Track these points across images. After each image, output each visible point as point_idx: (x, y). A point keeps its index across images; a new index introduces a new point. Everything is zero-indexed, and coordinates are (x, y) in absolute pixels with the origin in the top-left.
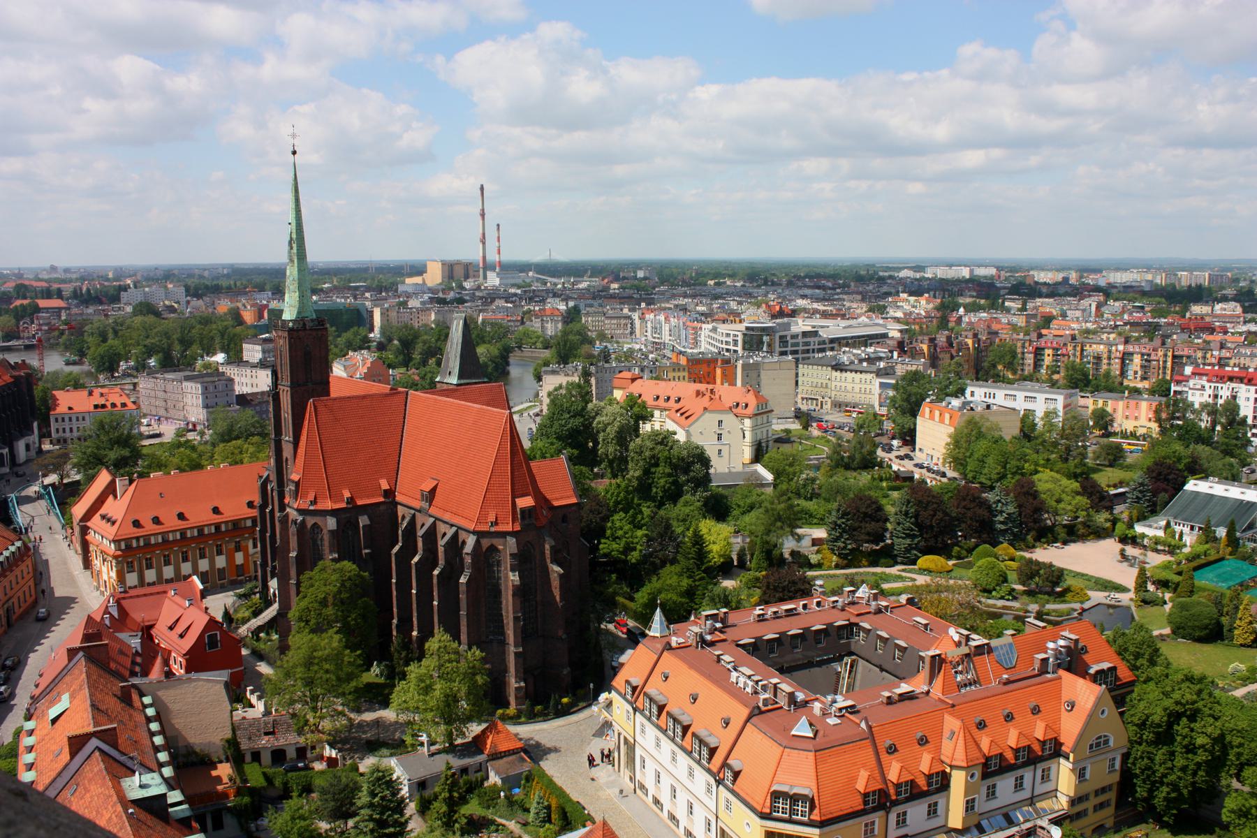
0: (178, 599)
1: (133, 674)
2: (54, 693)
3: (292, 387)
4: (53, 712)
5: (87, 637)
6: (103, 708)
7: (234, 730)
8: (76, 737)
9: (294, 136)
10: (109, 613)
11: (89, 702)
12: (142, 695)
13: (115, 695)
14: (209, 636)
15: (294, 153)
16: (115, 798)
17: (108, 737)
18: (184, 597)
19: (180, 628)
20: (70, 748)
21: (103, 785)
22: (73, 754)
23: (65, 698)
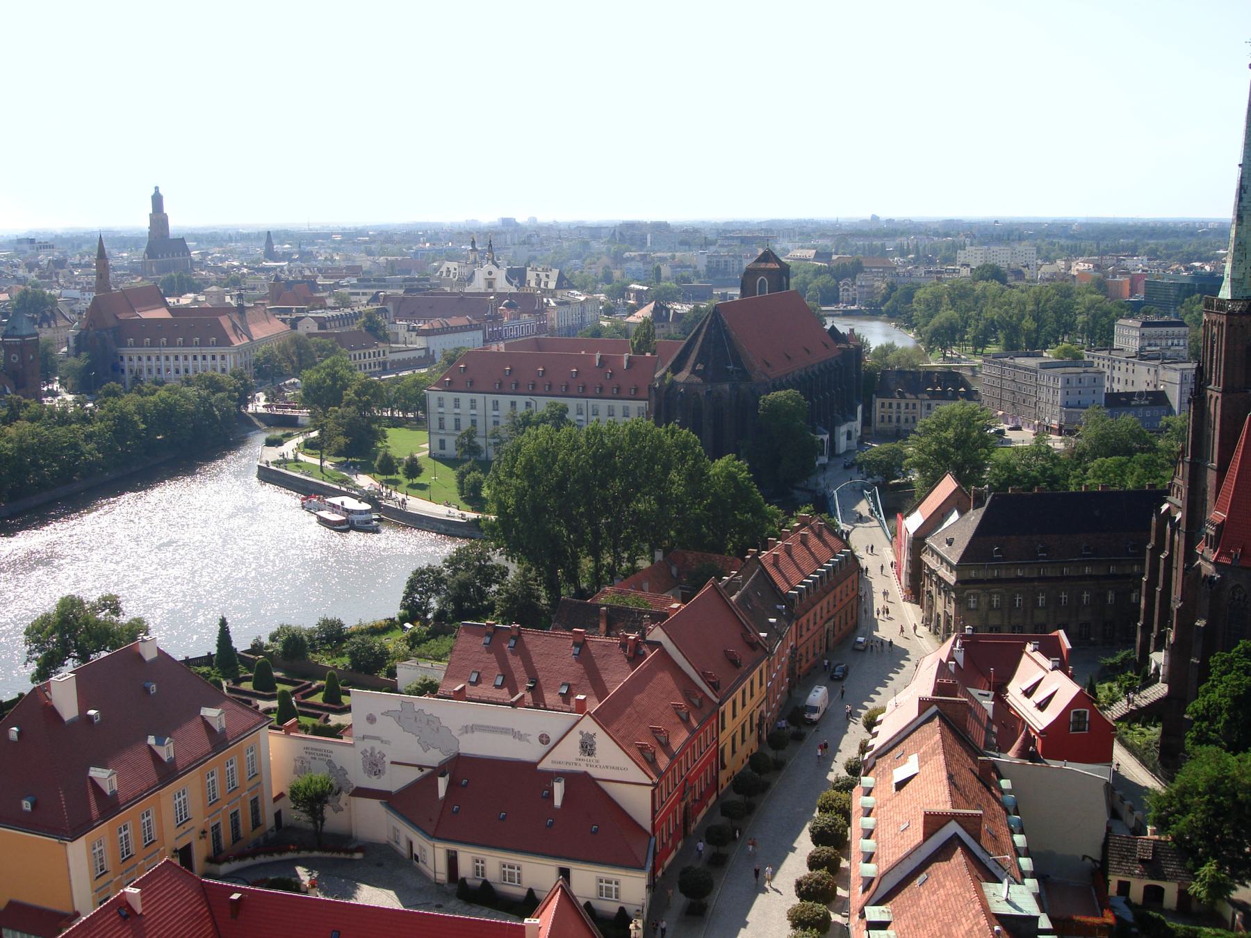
0: (1038, 656)
1: (988, 745)
2: (897, 751)
3: (1224, 392)
4: (900, 774)
5: (939, 689)
6: (960, 783)
7: (1105, 845)
8: (934, 815)
10: (954, 659)
11: (944, 774)
12: (1000, 777)
13: (972, 771)
14: (1074, 713)
16: (978, 907)
18: (1048, 655)
19: (1039, 696)
20: (925, 827)
21: (962, 885)
22: (927, 835)
23: (913, 760)
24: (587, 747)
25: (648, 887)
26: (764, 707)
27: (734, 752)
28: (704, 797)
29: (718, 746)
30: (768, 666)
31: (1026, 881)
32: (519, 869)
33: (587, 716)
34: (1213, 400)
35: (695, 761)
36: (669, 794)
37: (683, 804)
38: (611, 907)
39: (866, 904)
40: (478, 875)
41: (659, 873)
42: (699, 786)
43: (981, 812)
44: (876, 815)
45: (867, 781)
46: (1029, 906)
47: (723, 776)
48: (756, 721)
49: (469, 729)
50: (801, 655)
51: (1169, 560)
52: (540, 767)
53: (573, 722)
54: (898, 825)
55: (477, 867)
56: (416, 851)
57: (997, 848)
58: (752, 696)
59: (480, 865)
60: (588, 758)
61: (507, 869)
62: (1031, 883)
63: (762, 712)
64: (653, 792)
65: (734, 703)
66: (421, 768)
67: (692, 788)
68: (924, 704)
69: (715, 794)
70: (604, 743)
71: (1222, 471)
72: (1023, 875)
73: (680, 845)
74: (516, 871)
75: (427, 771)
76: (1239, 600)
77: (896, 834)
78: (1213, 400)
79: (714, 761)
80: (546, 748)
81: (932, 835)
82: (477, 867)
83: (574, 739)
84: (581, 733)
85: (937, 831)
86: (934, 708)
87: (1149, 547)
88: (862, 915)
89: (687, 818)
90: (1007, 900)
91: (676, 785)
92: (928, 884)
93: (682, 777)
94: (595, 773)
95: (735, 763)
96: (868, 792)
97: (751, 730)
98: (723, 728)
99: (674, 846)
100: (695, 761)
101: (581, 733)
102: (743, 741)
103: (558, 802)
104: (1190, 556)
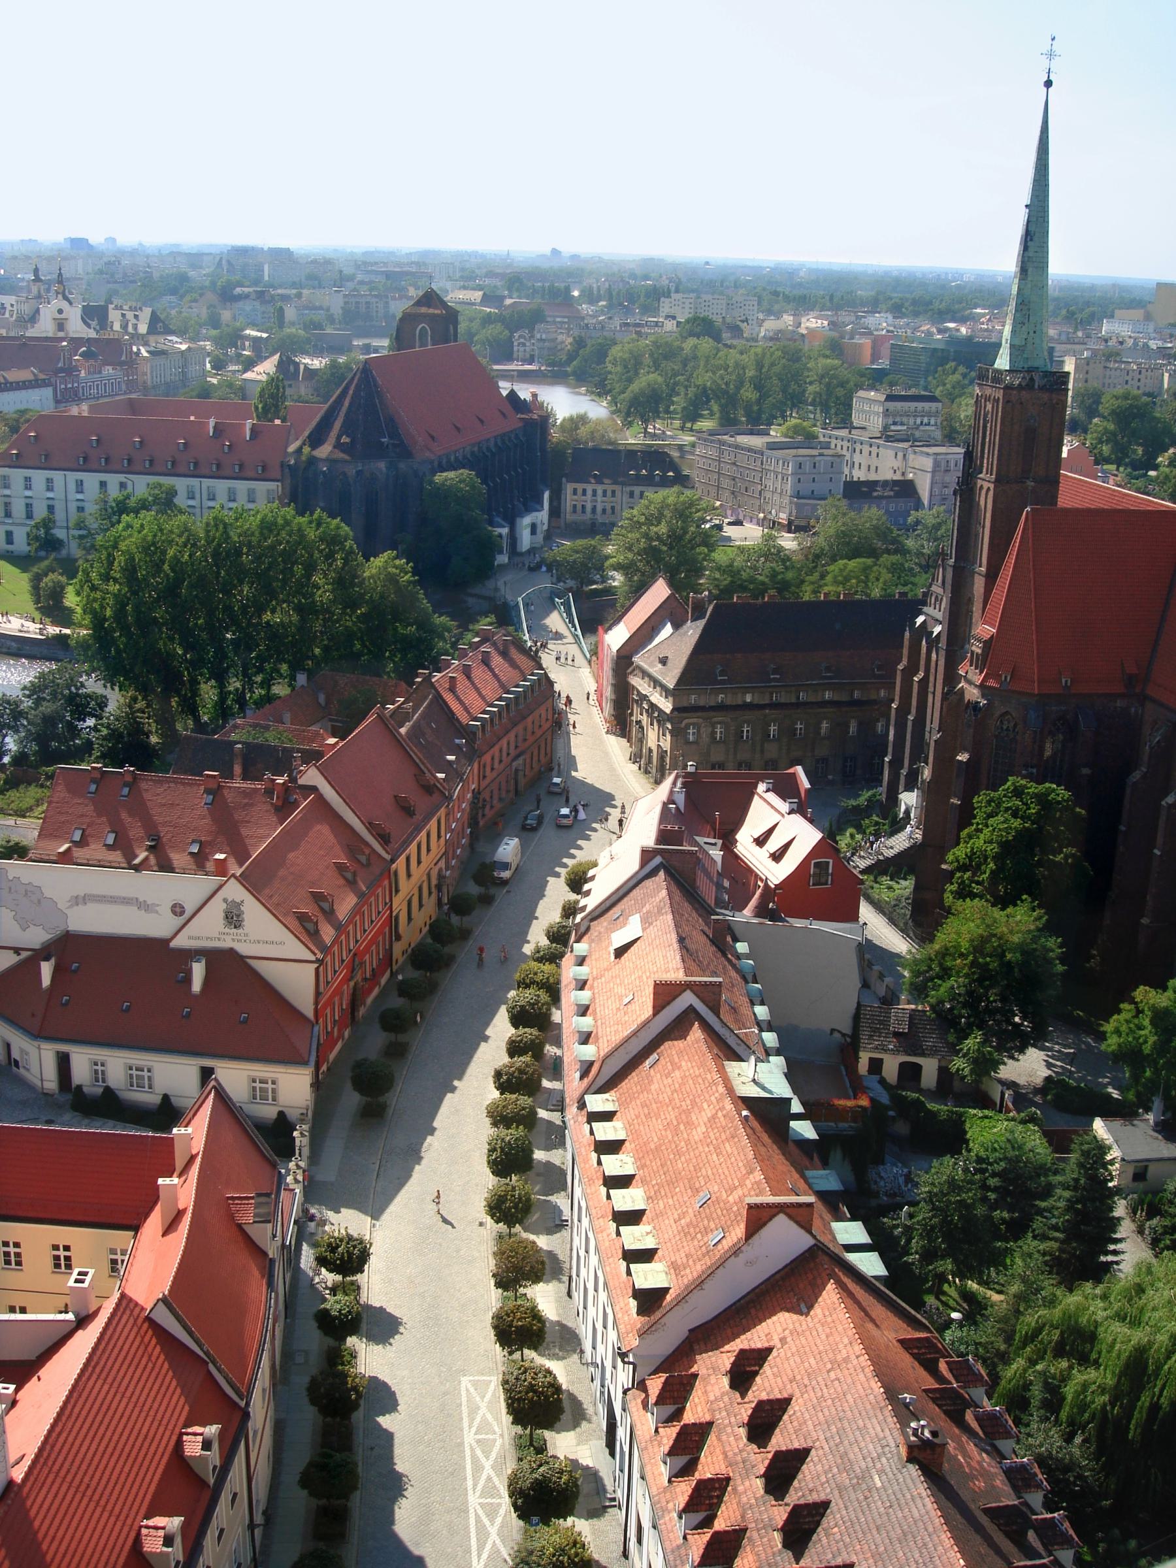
0: (772, 797)
1: (720, 903)
3: (997, 482)
4: (619, 938)
5: (664, 836)
6: (692, 947)
7: (857, 1018)
9: (1051, 55)
11: (673, 937)
12: (735, 940)
15: (1048, 84)
16: (721, 1089)
17: (710, 994)
18: (783, 796)
19: (774, 844)
21: (702, 1065)
22: (658, 1009)
23: (635, 922)
24: (233, 918)
25: (311, 1085)
26: (442, 864)
27: (410, 919)
28: (376, 974)
29: (391, 912)
30: (447, 815)
31: (771, 1058)
32: (149, 1071)
33: (233, 880)
34: (984, 492)
35: (365, 931)
36: (335, 972)
37: (352, 984)
38: (268, 1112)
39: (586, 1092)
40: (97, 1081)
41: (324, 1068)
42: (371, 961)
43: (721, 980)
44: (592, 988)
45: (580, 948)
46: (780, 1088)
47: (398, 948)
48: (434, 882)
49: (79, 900)
50: (484, 800)
51: (924, 682)
52: (174, 944)
53: (214, 887)
54: (621, 998)
55: (96, 1072)
56: (15, 1054)
57: (737, 1021)
58: (429, 850)
59: (99, 1068)
60: (235, 931)
61: (134, 1072)
62: (778, 1062)
63: (440, 870)
64: (317, 970)
65: (408, 859)
66: (17, 951)
67: (362, 963)
68: (647, 855)
69: (388, 972)
70: (253, 911)
71: (991, 577)
72: (768, 1052)
73: (347, 1034)
74: (146, 1074)
75: (24, 954)
76: (1007, 729)
77: (618, 1009)
78: (984, 492)
79: (387, 929)
80: (181, 920)
81: (663, 1007)
82: (96, 1072)
83: (217, 908)
84: (225, 900)
85: (668, 1003)
86: (658, 860)
87: (900, 667)
88: (582, 1105)
89: (354, 1004)
90: (754, 1080)
91: (343, 961)
92: (659, 1066)
93: (350, 951)
94: (243, 949)
95: (412, 933)
96: (581, 961)
97: (430, 893)
98: (397, 891)
99: (341, 1036)
100: (365, 931)
101: (225, 900)
102: (421, 906)
103: (197, 986)
104: (951, 677)
